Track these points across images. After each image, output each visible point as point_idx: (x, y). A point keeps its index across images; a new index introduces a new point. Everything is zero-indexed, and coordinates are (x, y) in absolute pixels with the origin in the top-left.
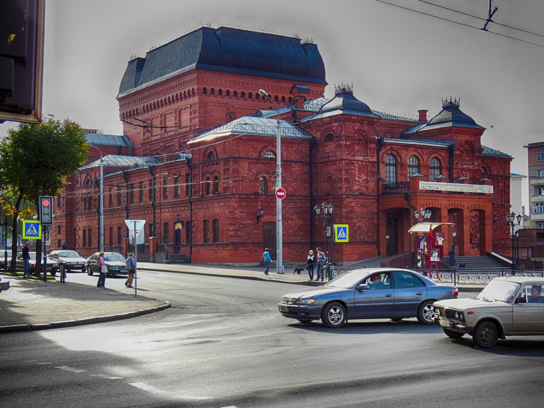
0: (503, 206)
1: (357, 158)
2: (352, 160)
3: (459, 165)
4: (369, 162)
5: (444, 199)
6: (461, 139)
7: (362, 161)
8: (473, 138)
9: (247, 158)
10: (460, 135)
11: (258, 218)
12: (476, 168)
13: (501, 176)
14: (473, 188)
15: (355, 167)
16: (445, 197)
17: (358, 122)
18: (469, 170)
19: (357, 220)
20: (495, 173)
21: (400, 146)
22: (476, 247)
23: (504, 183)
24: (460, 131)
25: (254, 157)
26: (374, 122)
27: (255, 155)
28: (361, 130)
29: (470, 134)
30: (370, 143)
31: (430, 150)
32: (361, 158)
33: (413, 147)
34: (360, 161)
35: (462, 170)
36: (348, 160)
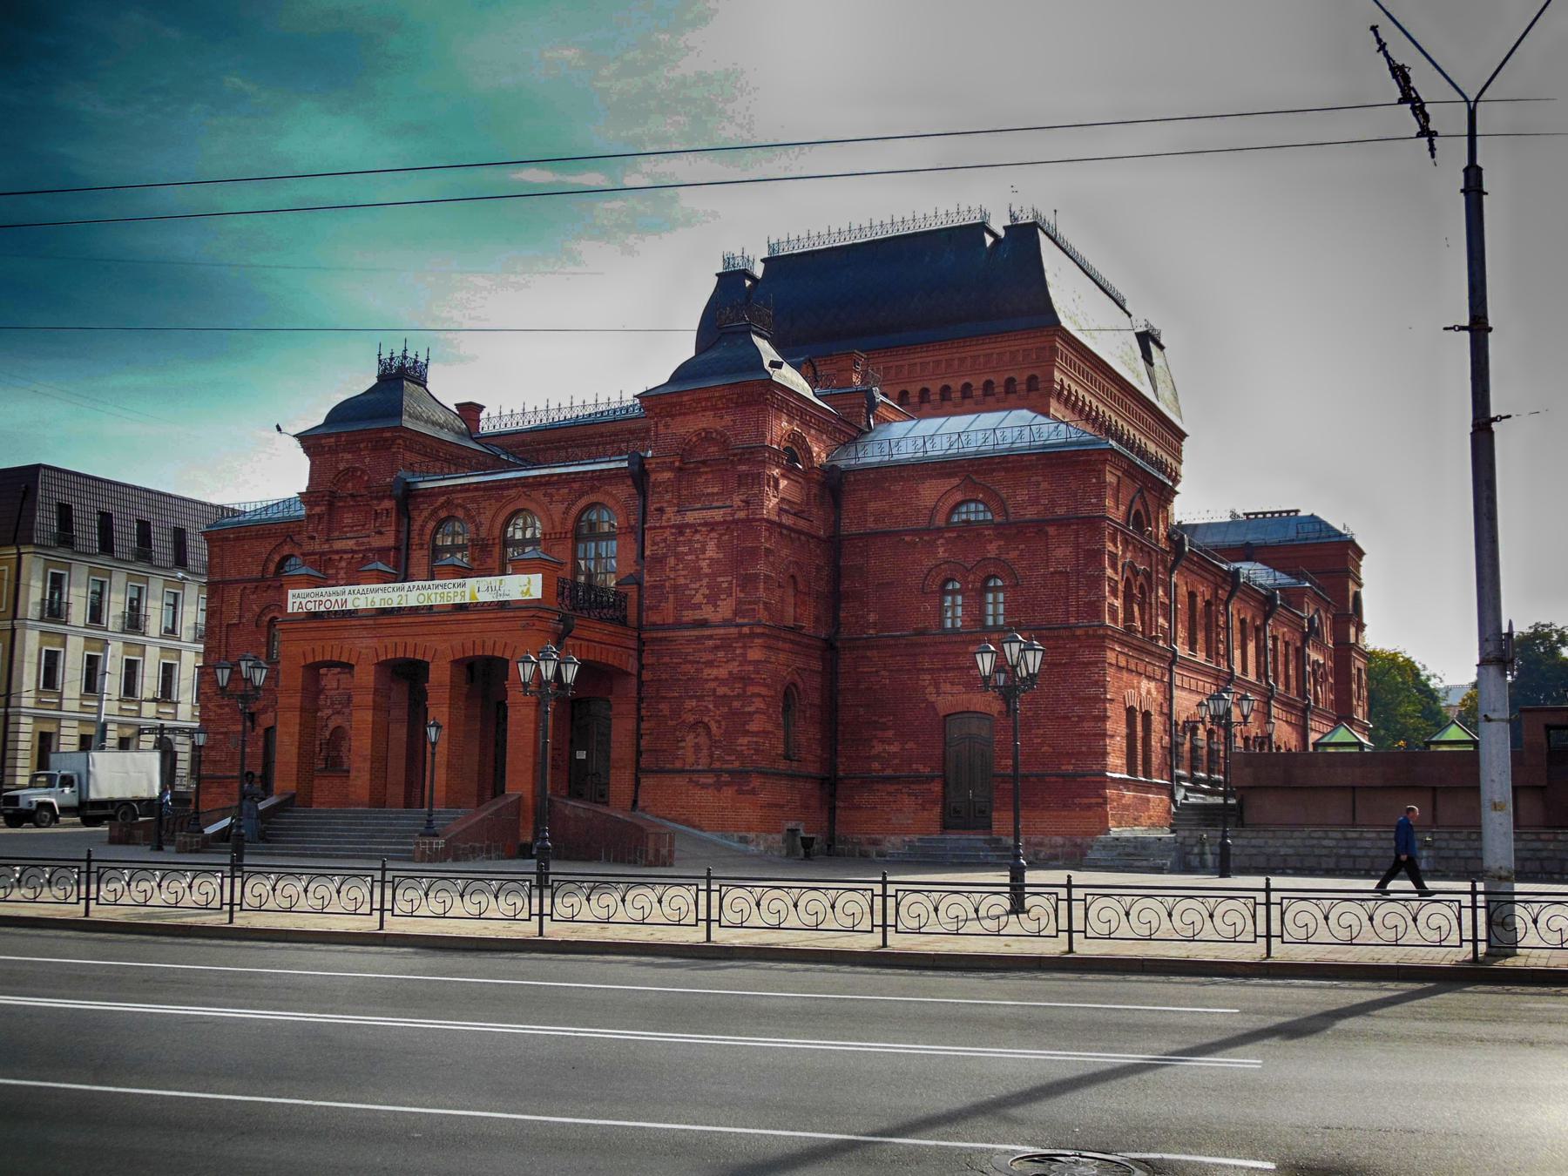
0: (1063, 633)
1: (338, 545)
2: (322, 554)
3: (670, 511)
4: (370, 550)
5: (365, 633)
6: (682, 431)
7: (353, 552)
8: (728, 418)
9: (237, 582)
10: (679, 419)
11: (252, 717)
12: (741, 515)
13: (1062, 523)
14: (467, 590)
15: (337, 568)
16: (365, 627)
17: (344, 451)
18: (712, 526)
19: (330, 712)
20: (1030, 513)
21: (476, 489)
22: (728, 784)
23: (1077, 546)
24: (673, 405)
25: (254, 575)
26: (386, 440)
27: (256, 574)
28: (355, 469)
29: (715, 408)
30: (377, 498)
31: (576, 486)
32: (350, 544)
33: (515, 486)
34: (345, 552)
35: (681, 529)
36: (313, 554)
